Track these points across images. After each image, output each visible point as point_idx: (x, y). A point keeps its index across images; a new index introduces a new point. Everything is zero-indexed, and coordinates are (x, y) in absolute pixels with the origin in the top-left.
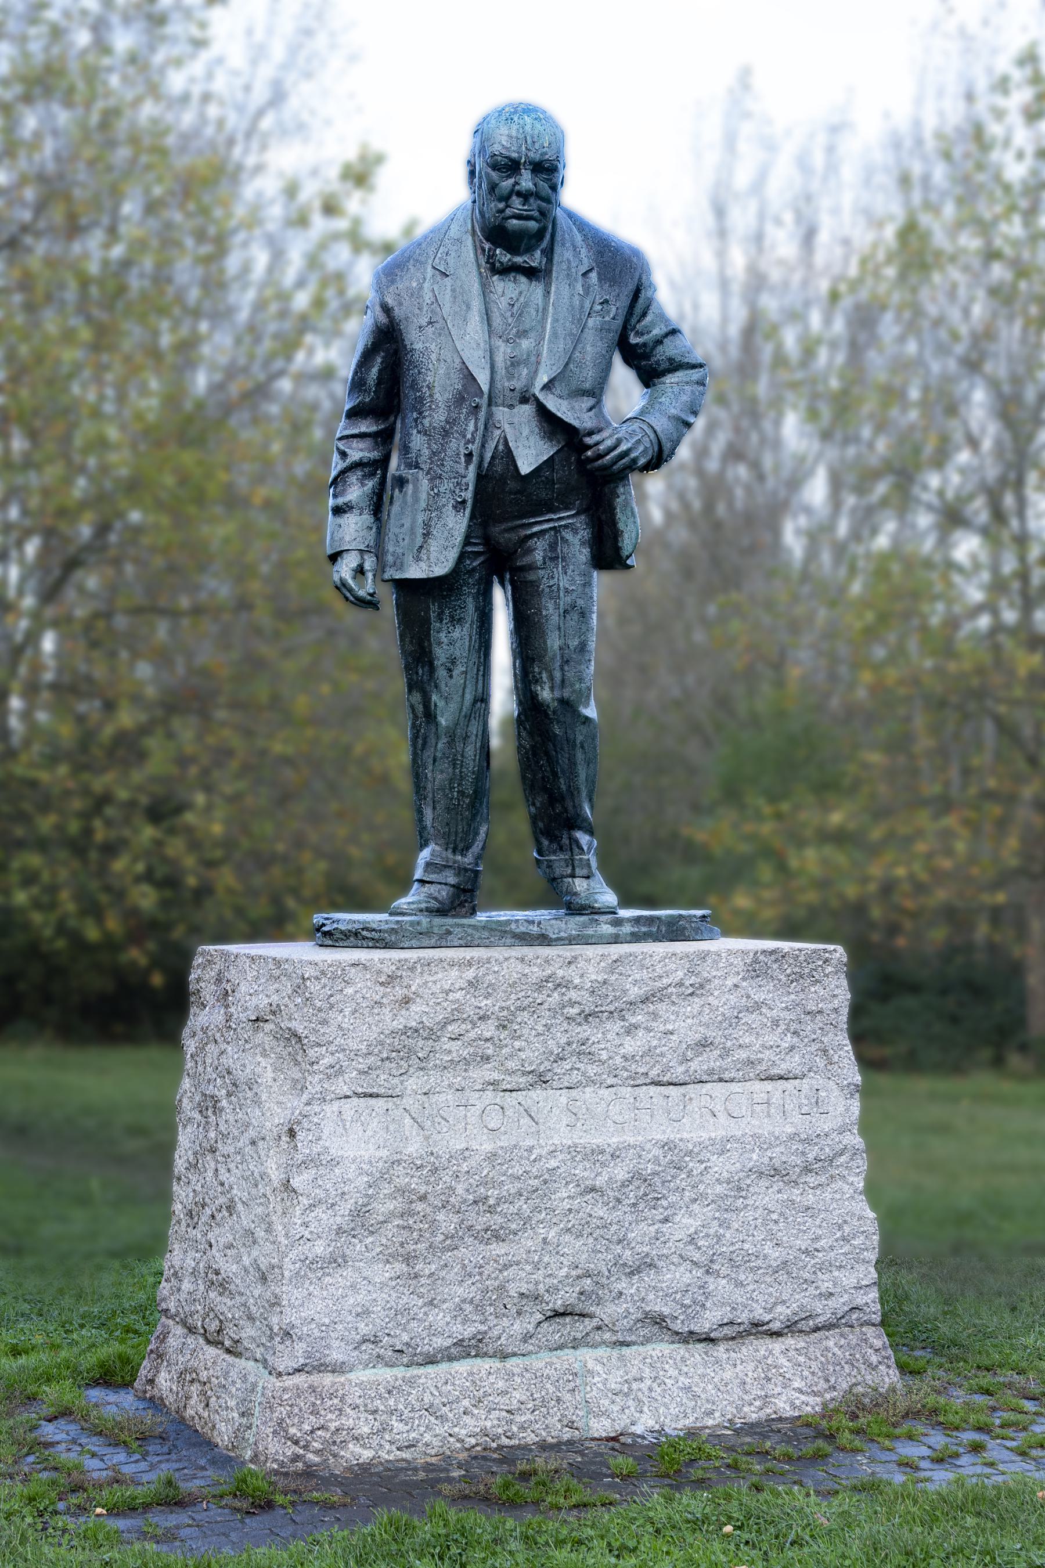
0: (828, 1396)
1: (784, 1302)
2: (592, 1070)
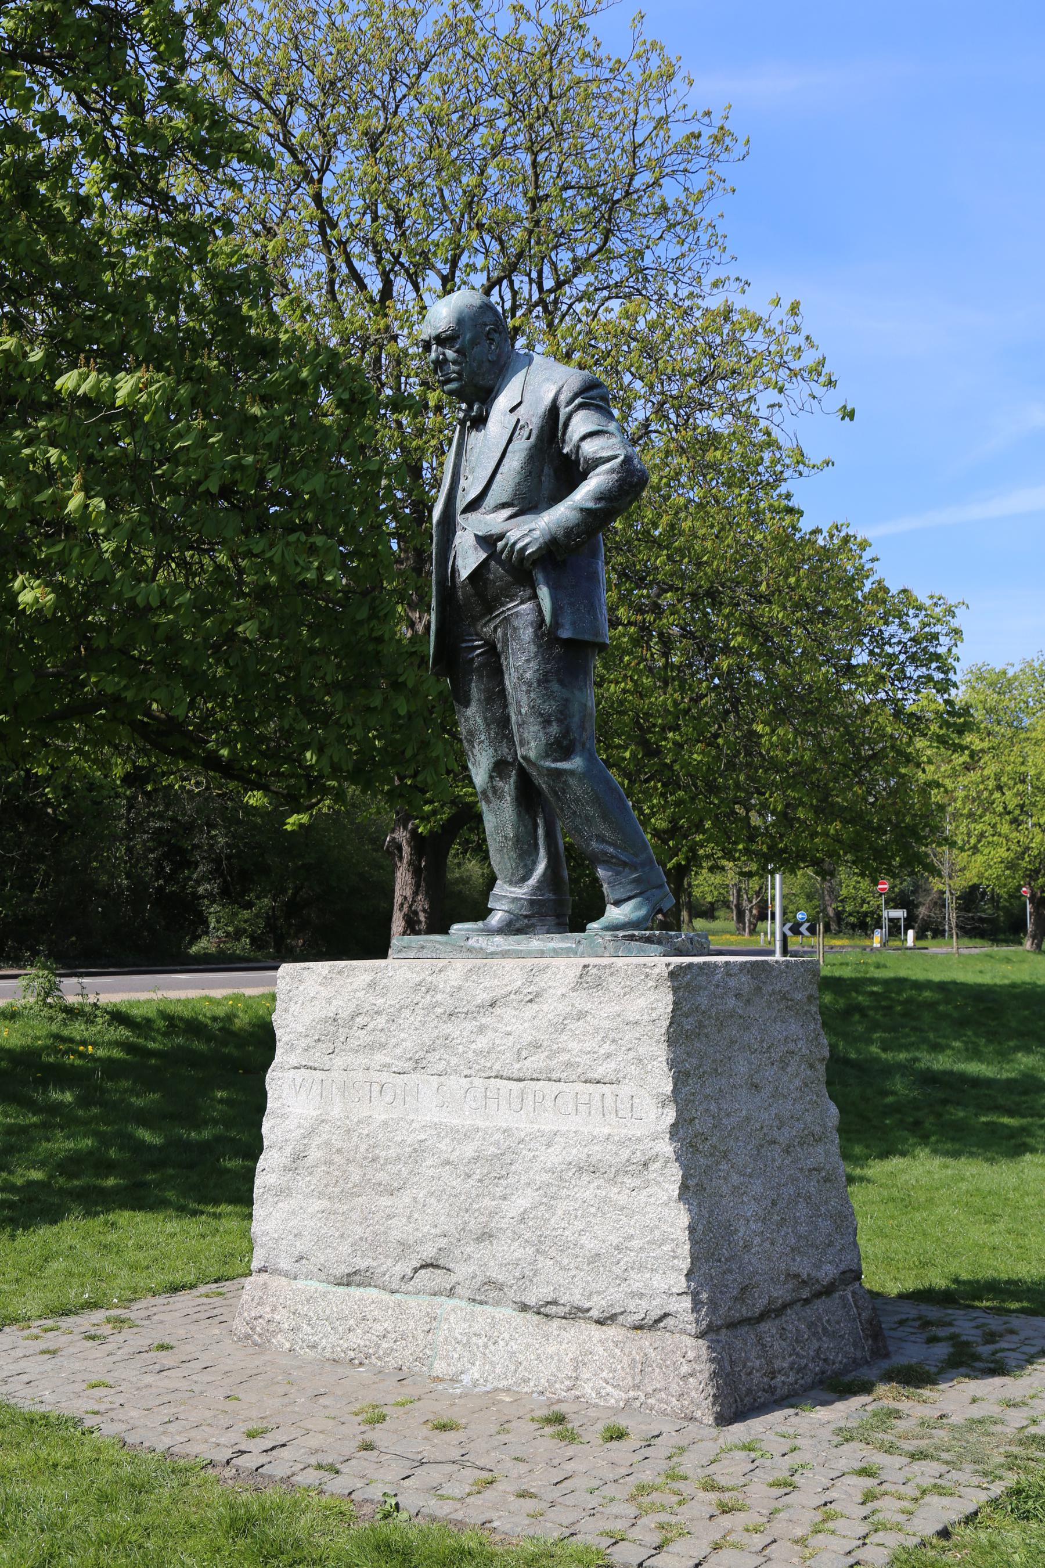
0: (632, 1394)
1: (598, 1293)
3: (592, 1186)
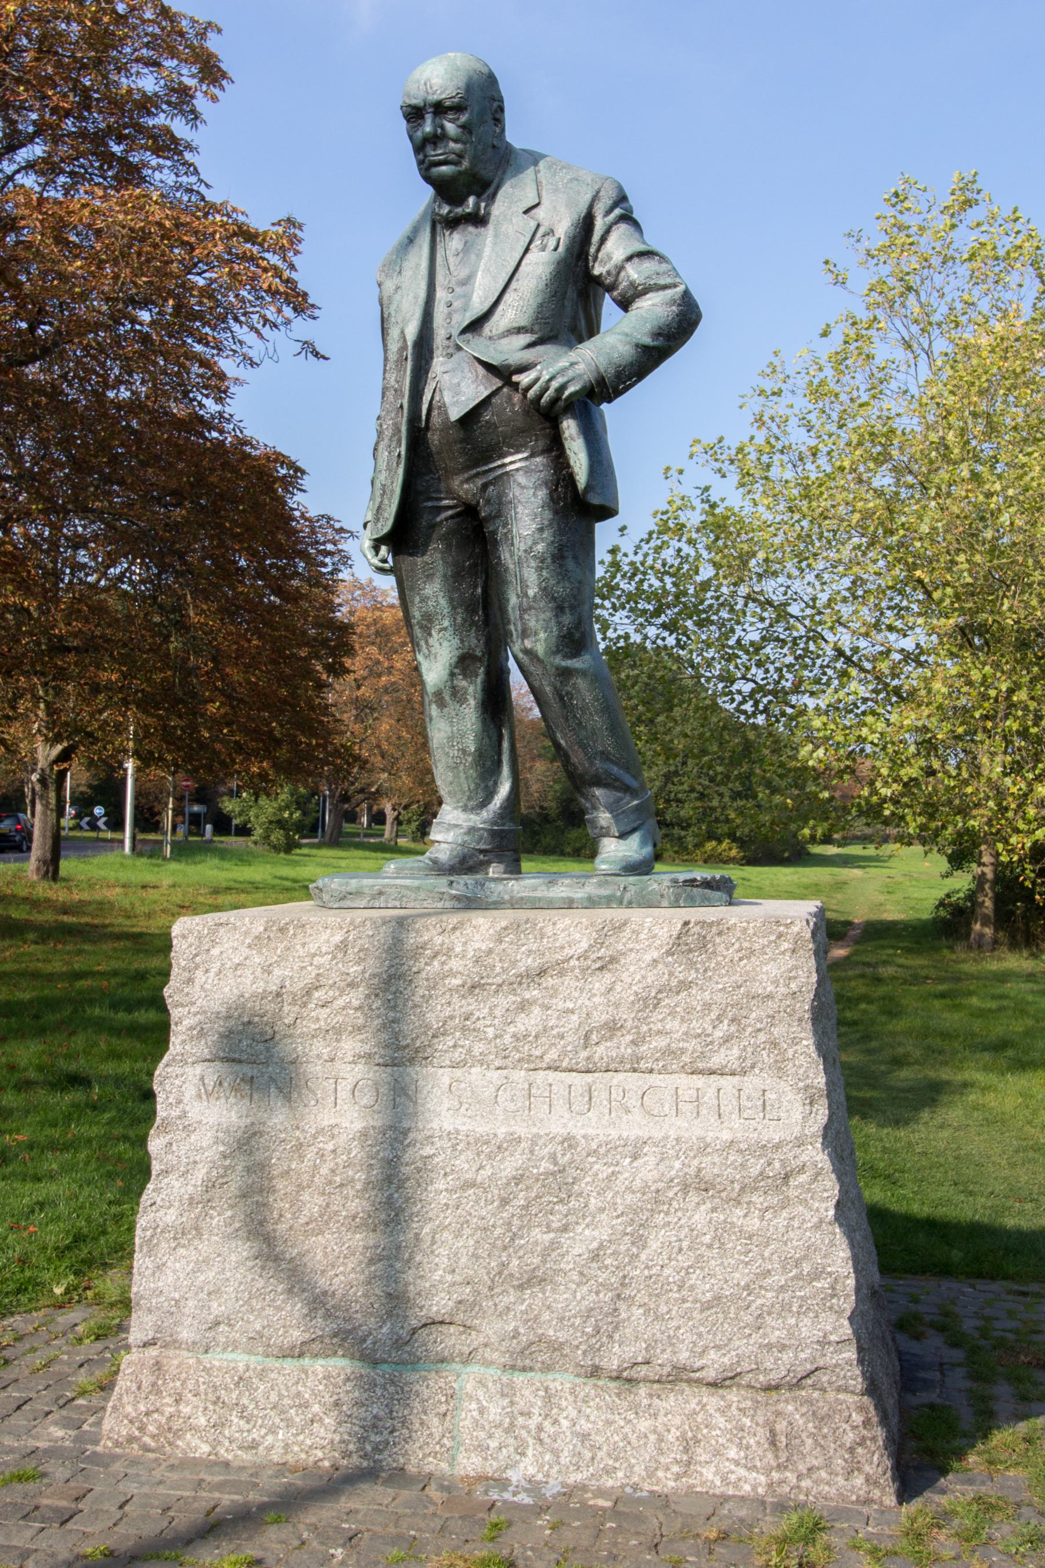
0: (775, 1475)
2: (478, 1048)
3: (703, 1208)
